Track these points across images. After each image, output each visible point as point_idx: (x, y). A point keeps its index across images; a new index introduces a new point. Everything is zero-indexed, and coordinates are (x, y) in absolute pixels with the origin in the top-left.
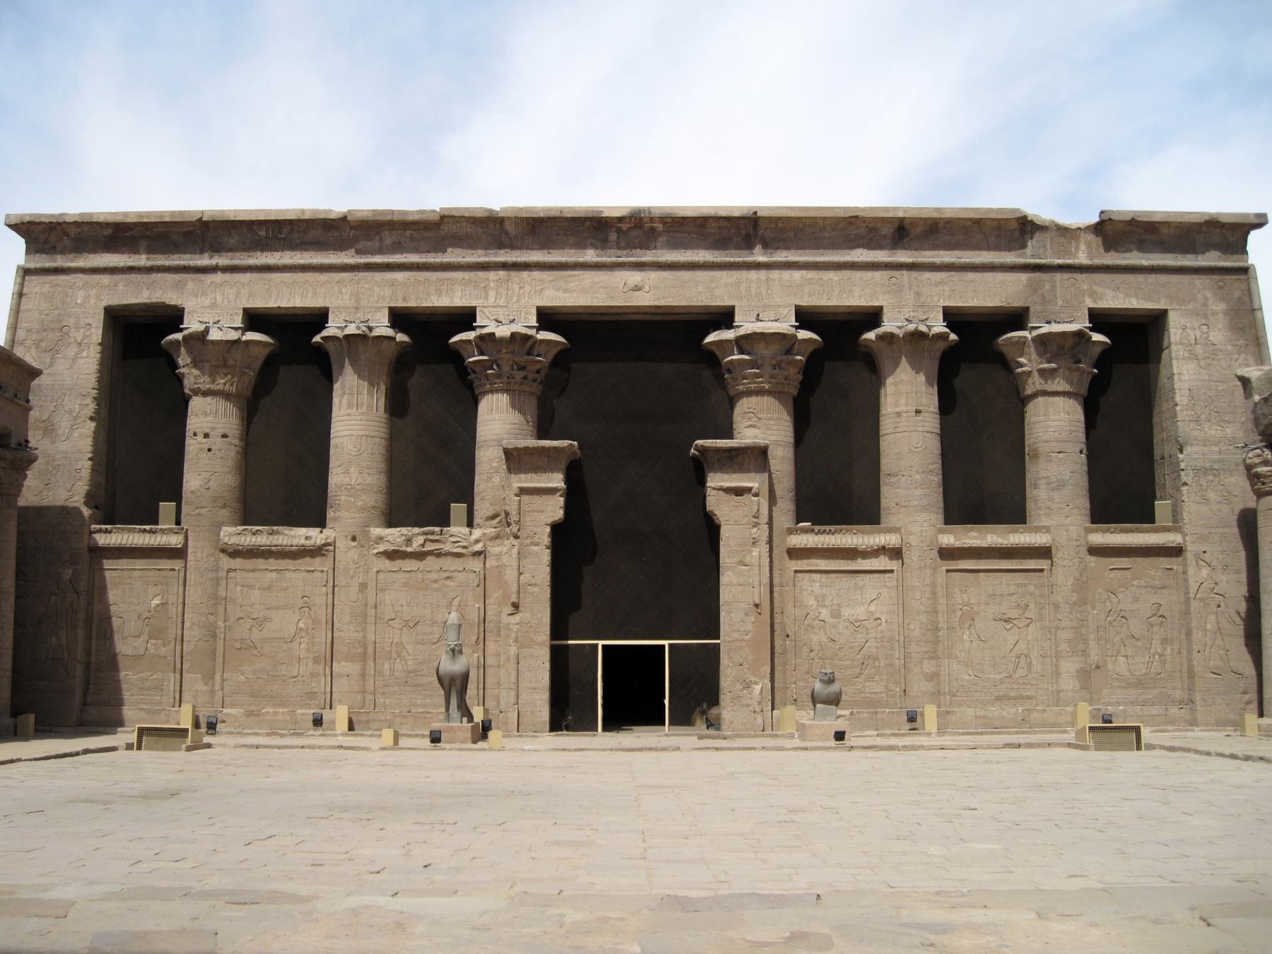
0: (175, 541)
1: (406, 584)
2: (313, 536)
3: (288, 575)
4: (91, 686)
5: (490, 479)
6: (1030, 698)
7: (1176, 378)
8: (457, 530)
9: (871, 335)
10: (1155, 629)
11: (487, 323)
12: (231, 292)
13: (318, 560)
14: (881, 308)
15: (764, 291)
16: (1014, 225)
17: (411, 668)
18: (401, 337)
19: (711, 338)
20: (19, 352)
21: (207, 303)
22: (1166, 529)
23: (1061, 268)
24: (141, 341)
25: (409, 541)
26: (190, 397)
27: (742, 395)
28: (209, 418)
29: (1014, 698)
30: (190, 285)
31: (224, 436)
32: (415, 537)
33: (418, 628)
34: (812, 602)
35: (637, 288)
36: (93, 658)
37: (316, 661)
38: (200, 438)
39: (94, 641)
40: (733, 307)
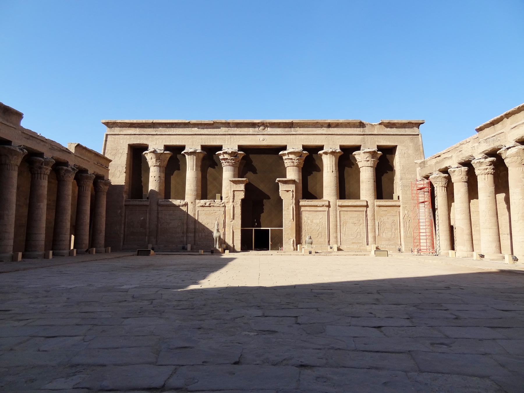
0: (147, 203)
1: (205, 214)
8: (218, 201)
16: (358, 124)
19: (281, 153)
20: (106, 156)
22: (396, 201)
24: (137, 152)
25: (205, 204)
30: (150, 139)
32: (208, 202)
34: (306, 219)
38: (153, 177)
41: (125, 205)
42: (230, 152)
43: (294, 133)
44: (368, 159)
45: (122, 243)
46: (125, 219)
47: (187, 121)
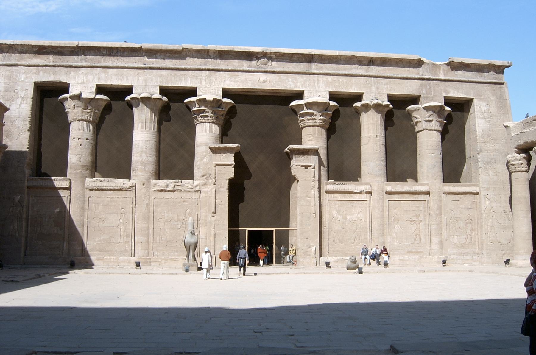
2: (120, 182)
3: (116, 199)
4: (28, 247)
5: (202, 160)
6: (420, 252)
7: (477, 125)
9: (358, 104)
10: (468, 225)
11: (201, 94)
12: (90, 77)
13: (128, 192)
14: (363, 93)
15: (316, 84)
17: (168, 239)
18: (165, 99)
19: (294, 103)
21: (80, 82)
23: (434, 80)
25: (167, 186)
26: (71, 122)
27: (302, 128)
28: (81, 132)
29: (414, 252)
30: (72, 73)
31: (87, 139)
32: (170, 183)
33: (171, 222)
34: (334, 213)
35: (265, 82)
36: (29, 235)
37: (127, 236)
38: (76, 140)
39: (29, 228)
40: (304, 91)
41: (28, 188)
42: (212, 99)
43: (316, 71)
44: (431, 119)
45: (22, 255)
46: (28, 211)
47: (137, 46)
